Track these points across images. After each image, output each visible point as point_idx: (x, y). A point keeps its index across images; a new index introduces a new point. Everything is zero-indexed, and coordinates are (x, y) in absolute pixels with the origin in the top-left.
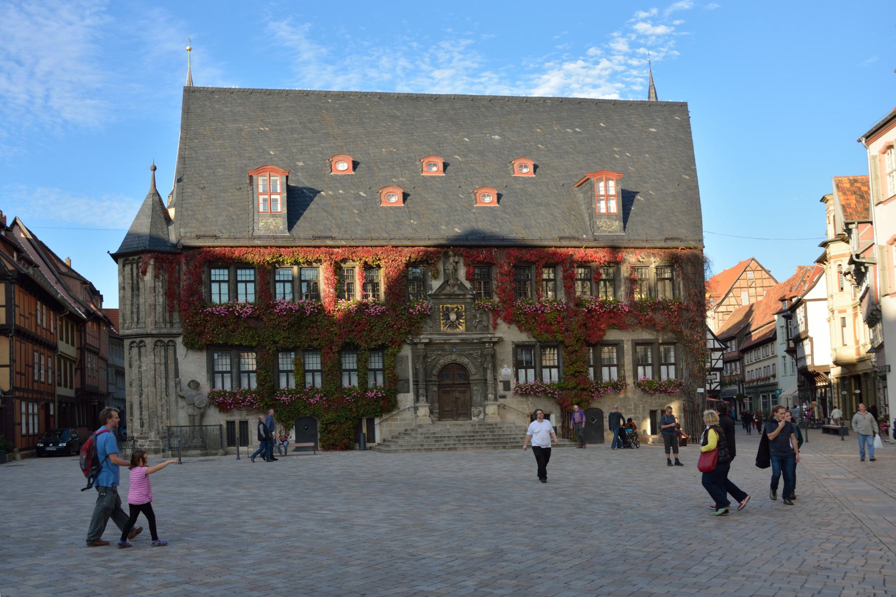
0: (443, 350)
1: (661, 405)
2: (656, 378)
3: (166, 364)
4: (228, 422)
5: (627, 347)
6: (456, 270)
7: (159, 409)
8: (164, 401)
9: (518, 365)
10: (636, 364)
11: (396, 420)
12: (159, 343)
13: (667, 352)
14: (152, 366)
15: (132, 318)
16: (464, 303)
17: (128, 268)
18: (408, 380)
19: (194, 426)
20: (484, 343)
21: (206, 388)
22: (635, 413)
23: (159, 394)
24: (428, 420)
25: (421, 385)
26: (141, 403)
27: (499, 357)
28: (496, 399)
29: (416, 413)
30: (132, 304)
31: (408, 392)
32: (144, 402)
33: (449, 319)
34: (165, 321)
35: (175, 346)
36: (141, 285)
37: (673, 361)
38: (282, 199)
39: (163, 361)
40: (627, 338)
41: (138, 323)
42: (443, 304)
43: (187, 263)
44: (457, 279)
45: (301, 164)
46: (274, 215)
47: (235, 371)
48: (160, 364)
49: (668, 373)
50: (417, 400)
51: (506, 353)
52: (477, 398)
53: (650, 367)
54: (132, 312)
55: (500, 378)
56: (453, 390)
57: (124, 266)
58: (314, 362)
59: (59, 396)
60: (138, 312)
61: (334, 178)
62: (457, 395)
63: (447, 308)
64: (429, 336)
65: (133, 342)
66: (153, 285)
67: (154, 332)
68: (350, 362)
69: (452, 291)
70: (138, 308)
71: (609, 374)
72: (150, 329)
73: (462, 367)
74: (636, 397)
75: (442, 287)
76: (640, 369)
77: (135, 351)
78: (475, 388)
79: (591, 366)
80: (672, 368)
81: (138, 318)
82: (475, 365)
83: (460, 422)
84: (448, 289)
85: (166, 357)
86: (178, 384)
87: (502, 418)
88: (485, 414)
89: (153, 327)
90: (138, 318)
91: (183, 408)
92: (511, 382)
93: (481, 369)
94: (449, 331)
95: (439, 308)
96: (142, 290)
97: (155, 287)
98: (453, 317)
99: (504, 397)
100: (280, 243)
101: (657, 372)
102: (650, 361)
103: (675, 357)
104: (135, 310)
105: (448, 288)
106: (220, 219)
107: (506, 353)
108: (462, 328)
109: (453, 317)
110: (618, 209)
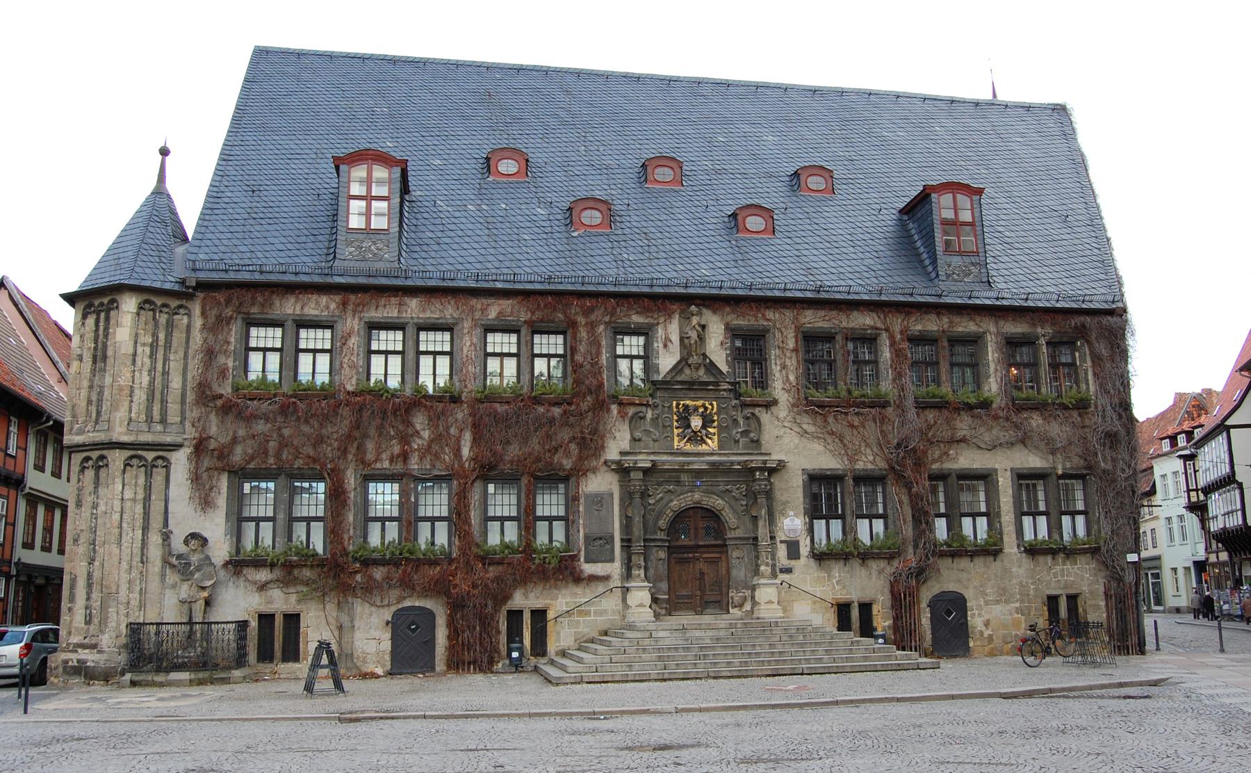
0: (678, 482)
1: (1066, 587)
2: (1056, 537)
3: (147, 499)
4: (262, 617)
5: (1005, 483)
6: (701, 338)
7: (124, 588)
8: (135, 573)
9: (813, 513)
10: (1020, 514)
11: (588, 613)
12: (135, 462)
13: (1069, 491)
14: (117, 504)
15: (88, 412)
16: (716, 399)
17: (91, 321)
18: (612, 537)
19: (190, 623)
20: (752, 470)
21: (220, 550)
22: (1022, 601)
23: (126, 558)
24: (647, 614)
25: (638, 546)
26: (90, 576)
27: (780, 496)
28: (774, 576)
29: (624, 600)
30: (91, 387)
31: (612, 560)
32: (97, 575)
33: (689, 426)
34: (149, 420)
35: (167, 467)
36: (110, 353)
37: (1080, 506)
39: (141, 496)
40: (1005, 463)
41: (97, 422)
42: (679, 399)
43: (203, 314)
44: (704, 355)
47: (281, 516)
48: (134, 500)
49: (1075, 528)
50: (628, 575)
51: (792, 489)
52: (739, 573)
53: (1044, 518)
54: (89, 402)
55: (781, 536)
56: (694, 554)
57: (84, 317)
58: (436, 502)
59: (18, 563)
60: (100, 401)
62: (701, 565)
63: (686, 407)
64: (652, 458)
65: (87, 459)
66: (131, 351)
67: (126, 439)
68: (503, 502)
69: (695, 376)
70: (101, 394)
71: (975, 529)
72: (120, 433)
73: (712, 515)
74: (1021, 571)
75: (677, 369)
76: (1027, 521)
77: (90, 474)
78: (735, 554)
79: (940, 515)
80: (1080, 520)
81: (99, 413)
82: (735, 511)
83: (707, 619)
84: (687, 374)
85: (148, 488)
86: (166, 537)
87: (785, 610)
88: (755, 603)
89: (123, 429)
90: (99, 413)
91: (174, 586)
92: (802, 544)
93: (747, 519)
94: (689, 447)
95: (670, 407)
96: (110, 361)
97: (135, 355)
98: (696, 422)
99: (788, 571)
101: (1054, 527)
102: (1042, 507)
103: (1085, 500)
104: (94, 398)
105: (687, 371)
107: (792, 489)
108: (712, 444)
109: (696, 422)
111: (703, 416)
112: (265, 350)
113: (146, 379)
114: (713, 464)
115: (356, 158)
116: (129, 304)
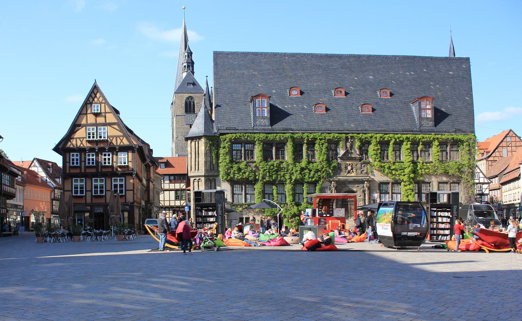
4: (240, 218)
17: (193, 143)
38: (267, 110)
45: (274, 91)
46: (264, 118)
47: (243, 193)
54: (195, 165)
61: (291, 99)
65: (195, 179)
98: (349, 168)
100: (267, 131)
106: (237, 119)
109: (349, 168)
110: (432, 116)
111: (352, 167)
112: (237, 150)
113: (209, 159)
114: (354, 180)
115: (257, 96)
116: (203, 140)
